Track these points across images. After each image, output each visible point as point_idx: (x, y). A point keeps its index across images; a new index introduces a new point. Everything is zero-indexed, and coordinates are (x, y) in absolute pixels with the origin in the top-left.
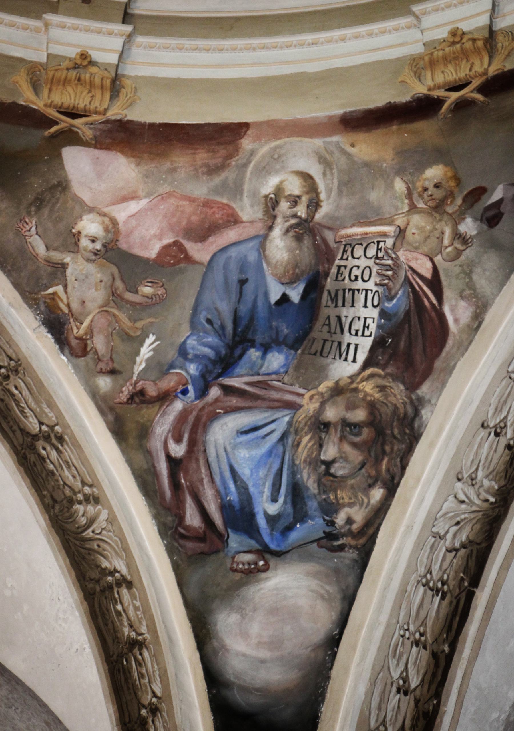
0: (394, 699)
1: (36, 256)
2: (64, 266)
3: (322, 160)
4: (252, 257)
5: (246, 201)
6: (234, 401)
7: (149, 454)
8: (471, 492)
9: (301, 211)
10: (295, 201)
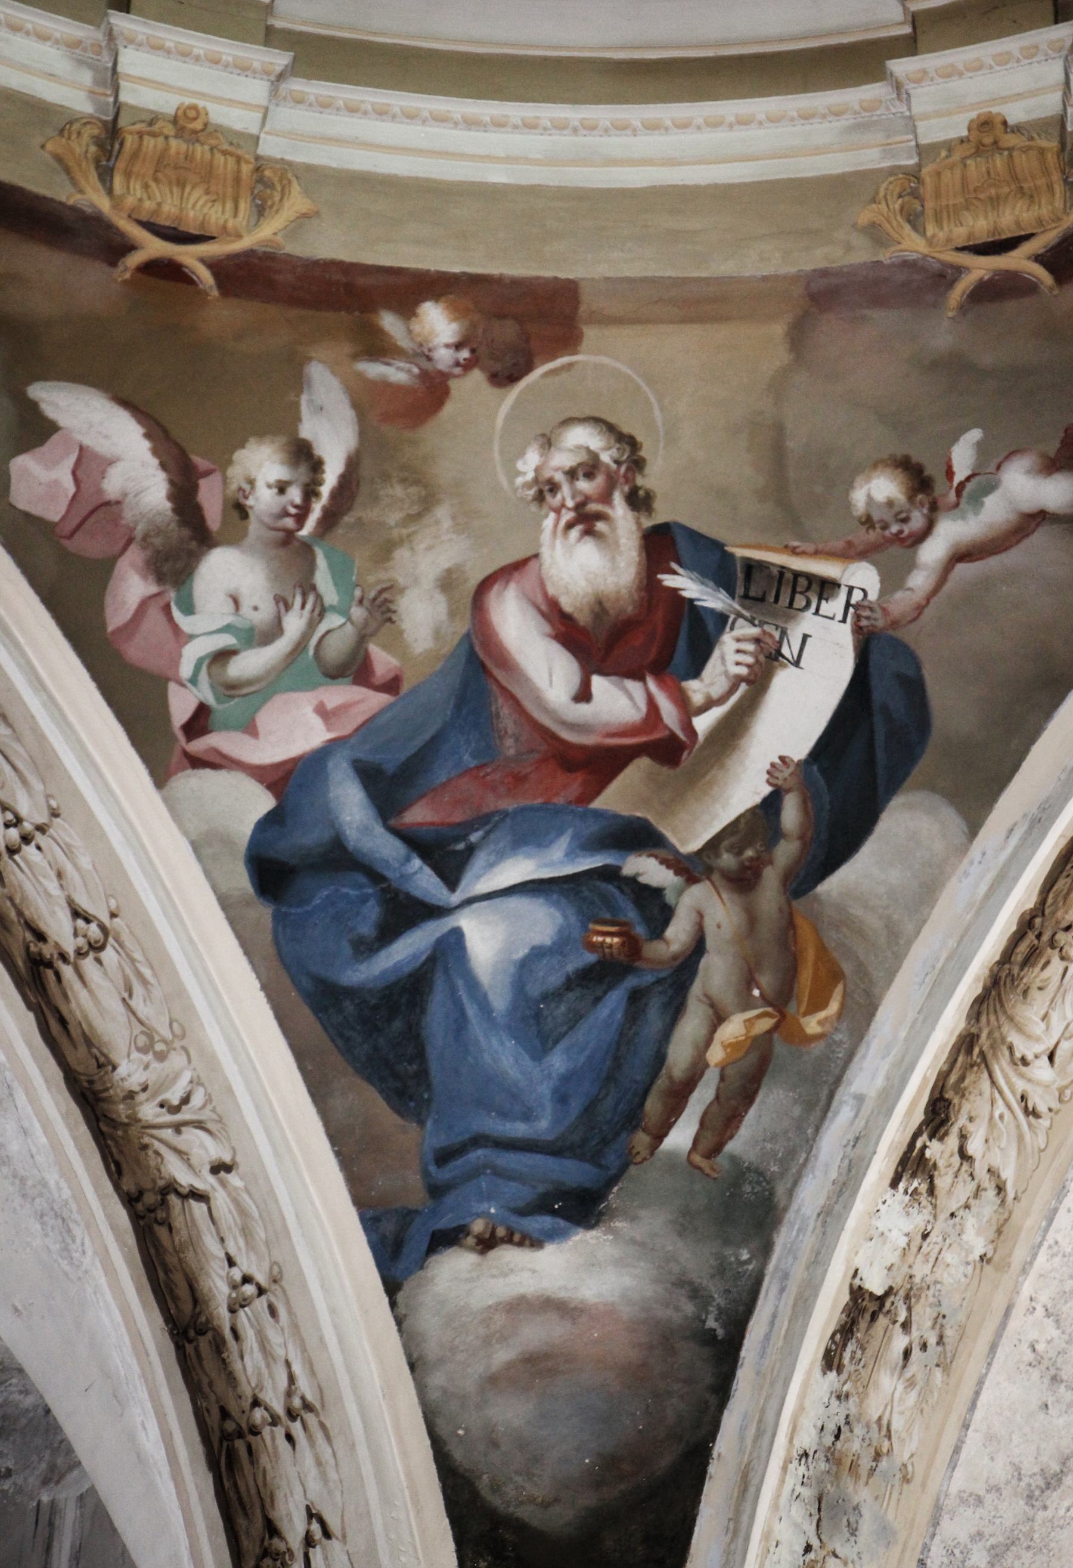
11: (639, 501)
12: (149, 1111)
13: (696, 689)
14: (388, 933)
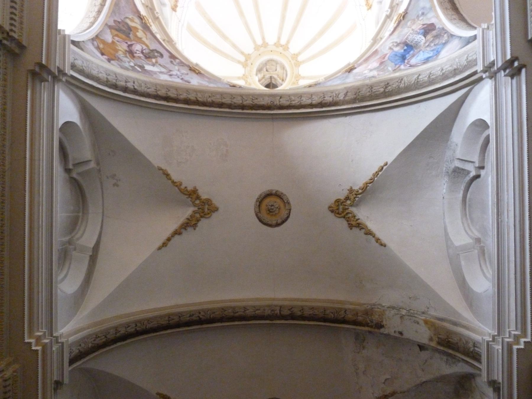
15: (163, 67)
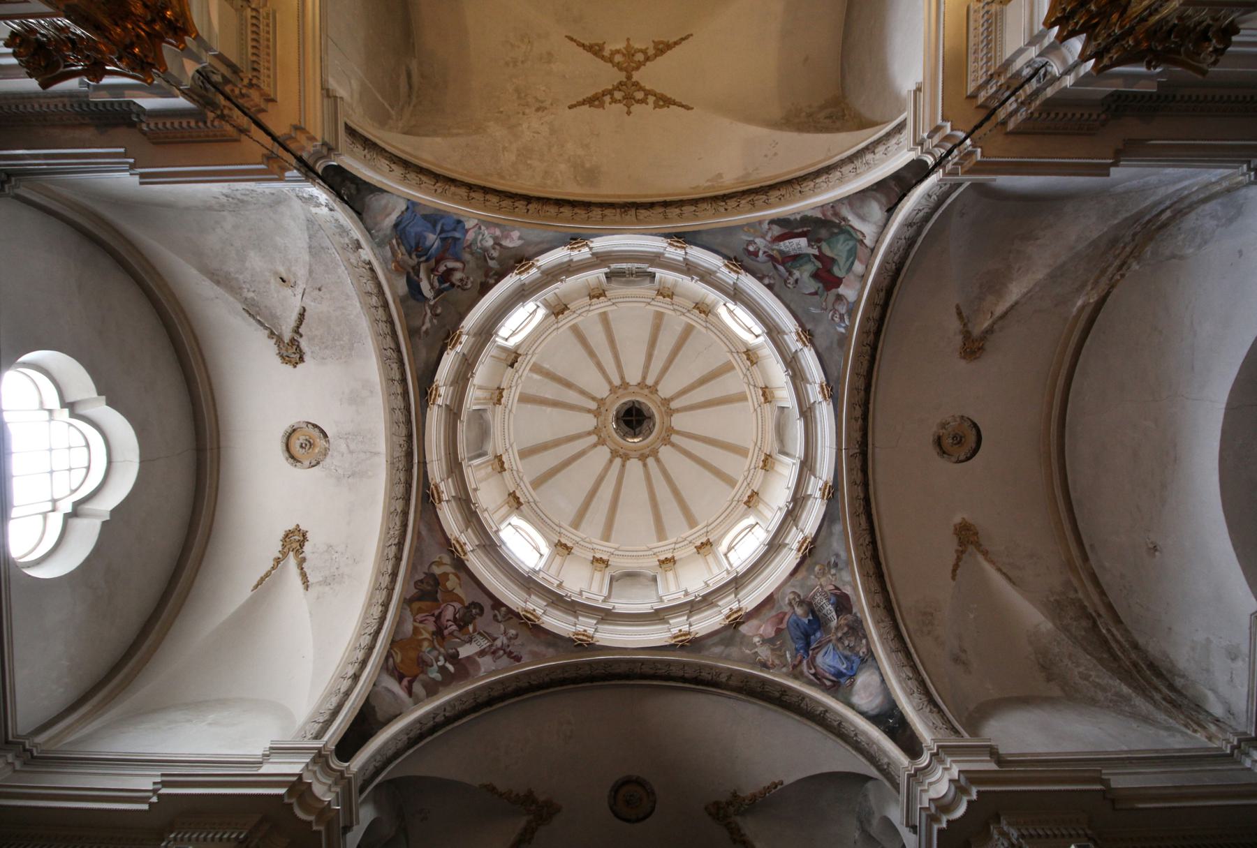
0: (909, 682)
1: (749, 655)
2: (756, 652)
3: (794, 586)
4: (795, 618)
5: (785, 608)
6: (816, 651)
7: (807, 677)
8: (885, 624)
9: (797, 600)
10: (794, 599)
11: (459, 286)
12: (447, 187)
13: (436, 278)
14: (442, 228)
15: (485, 637)
